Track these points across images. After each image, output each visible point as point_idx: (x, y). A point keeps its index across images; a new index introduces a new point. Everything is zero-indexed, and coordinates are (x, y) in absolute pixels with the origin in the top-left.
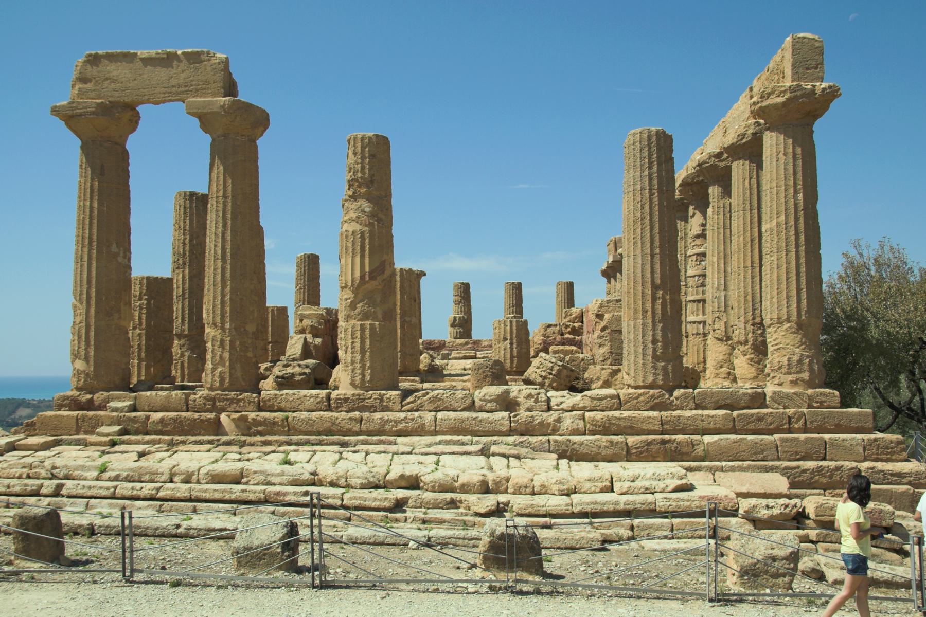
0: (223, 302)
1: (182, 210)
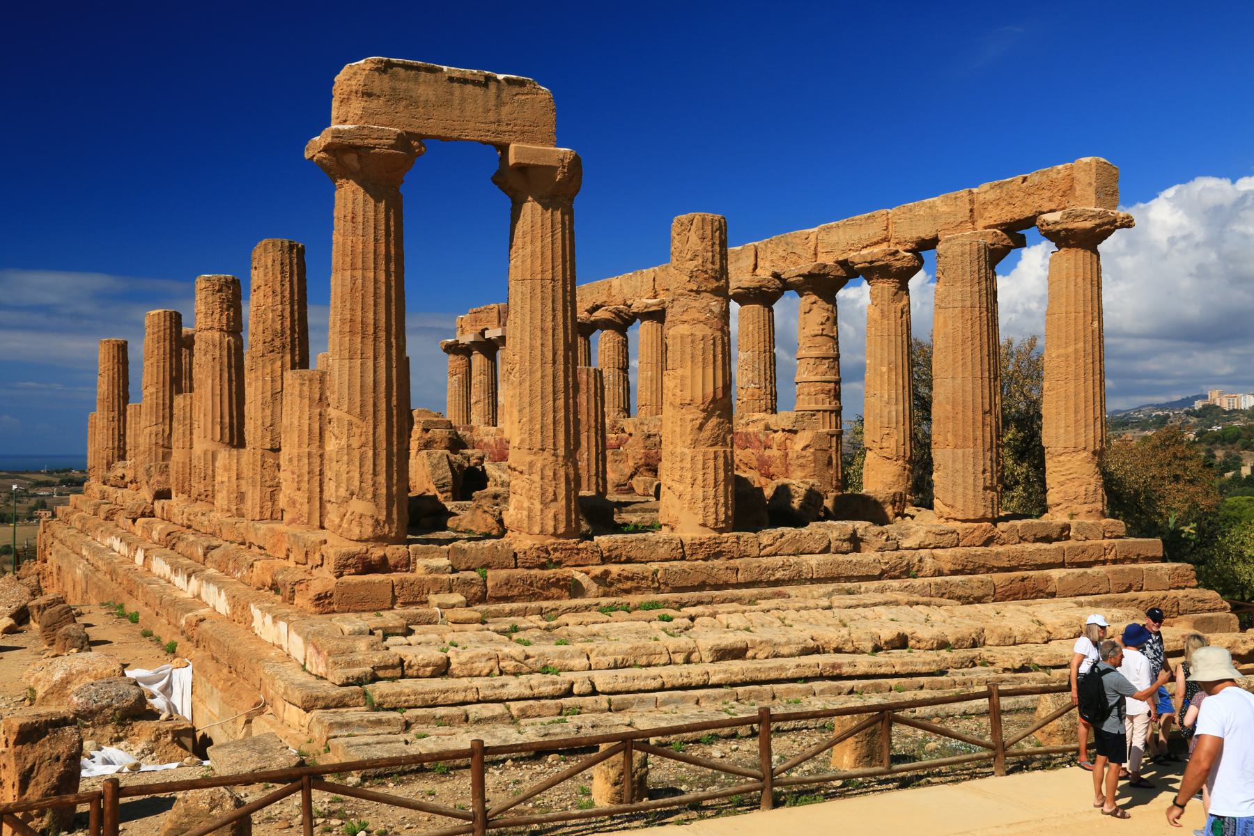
0: (555, 422)
1: (278, 267)
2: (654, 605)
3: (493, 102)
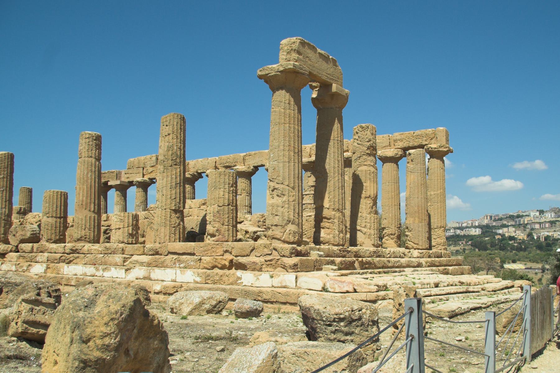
1: (179, 126)
2: (380, 273)
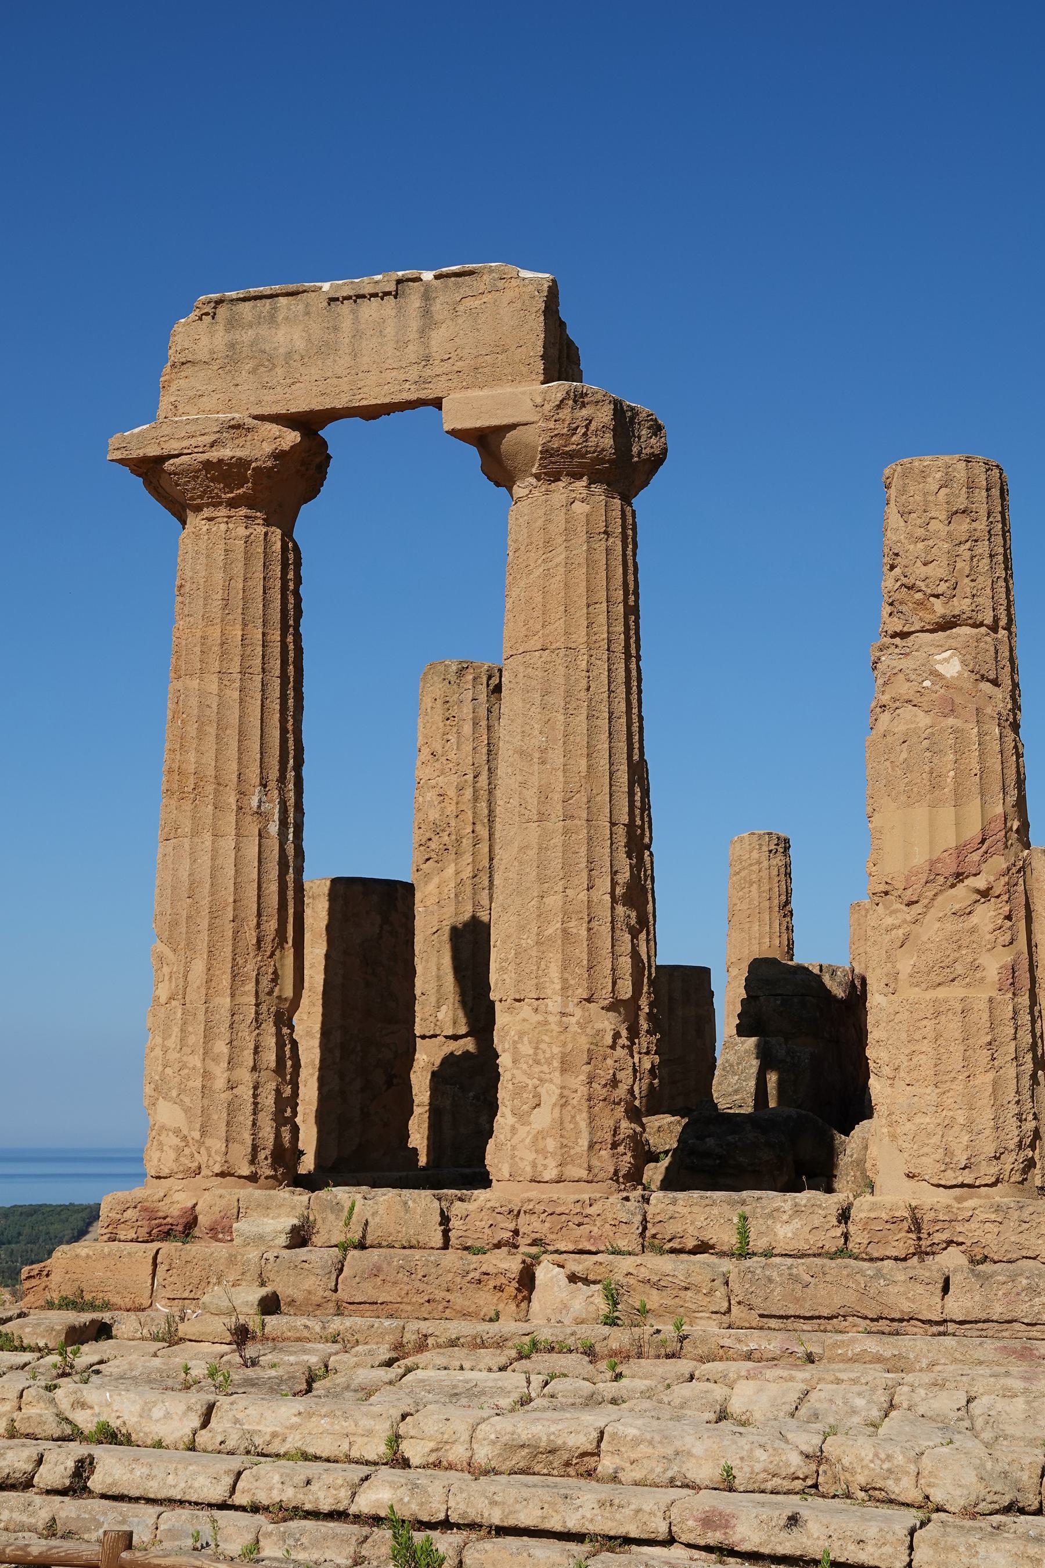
3: (415, 325)
